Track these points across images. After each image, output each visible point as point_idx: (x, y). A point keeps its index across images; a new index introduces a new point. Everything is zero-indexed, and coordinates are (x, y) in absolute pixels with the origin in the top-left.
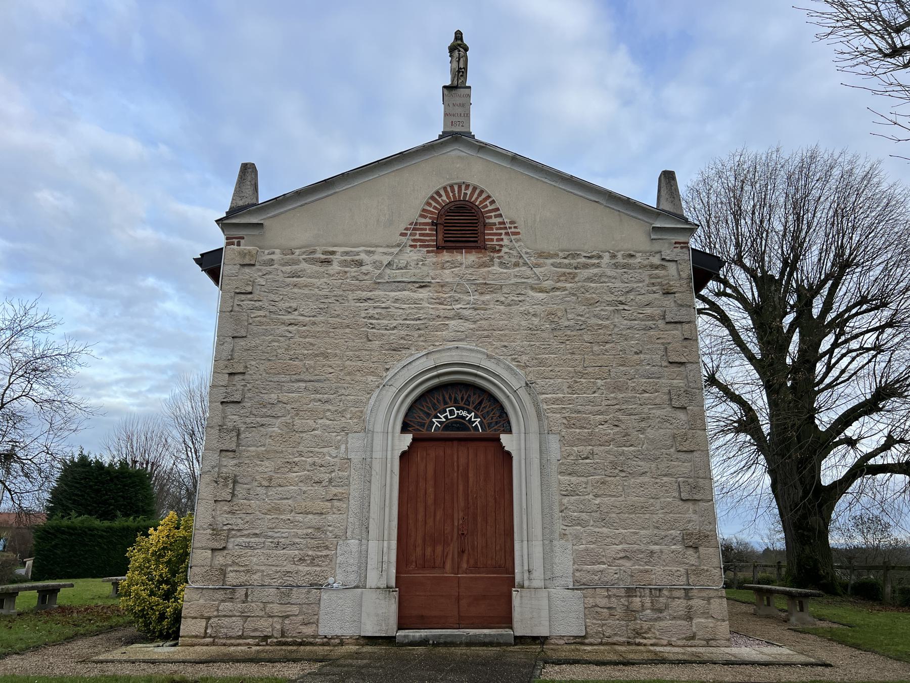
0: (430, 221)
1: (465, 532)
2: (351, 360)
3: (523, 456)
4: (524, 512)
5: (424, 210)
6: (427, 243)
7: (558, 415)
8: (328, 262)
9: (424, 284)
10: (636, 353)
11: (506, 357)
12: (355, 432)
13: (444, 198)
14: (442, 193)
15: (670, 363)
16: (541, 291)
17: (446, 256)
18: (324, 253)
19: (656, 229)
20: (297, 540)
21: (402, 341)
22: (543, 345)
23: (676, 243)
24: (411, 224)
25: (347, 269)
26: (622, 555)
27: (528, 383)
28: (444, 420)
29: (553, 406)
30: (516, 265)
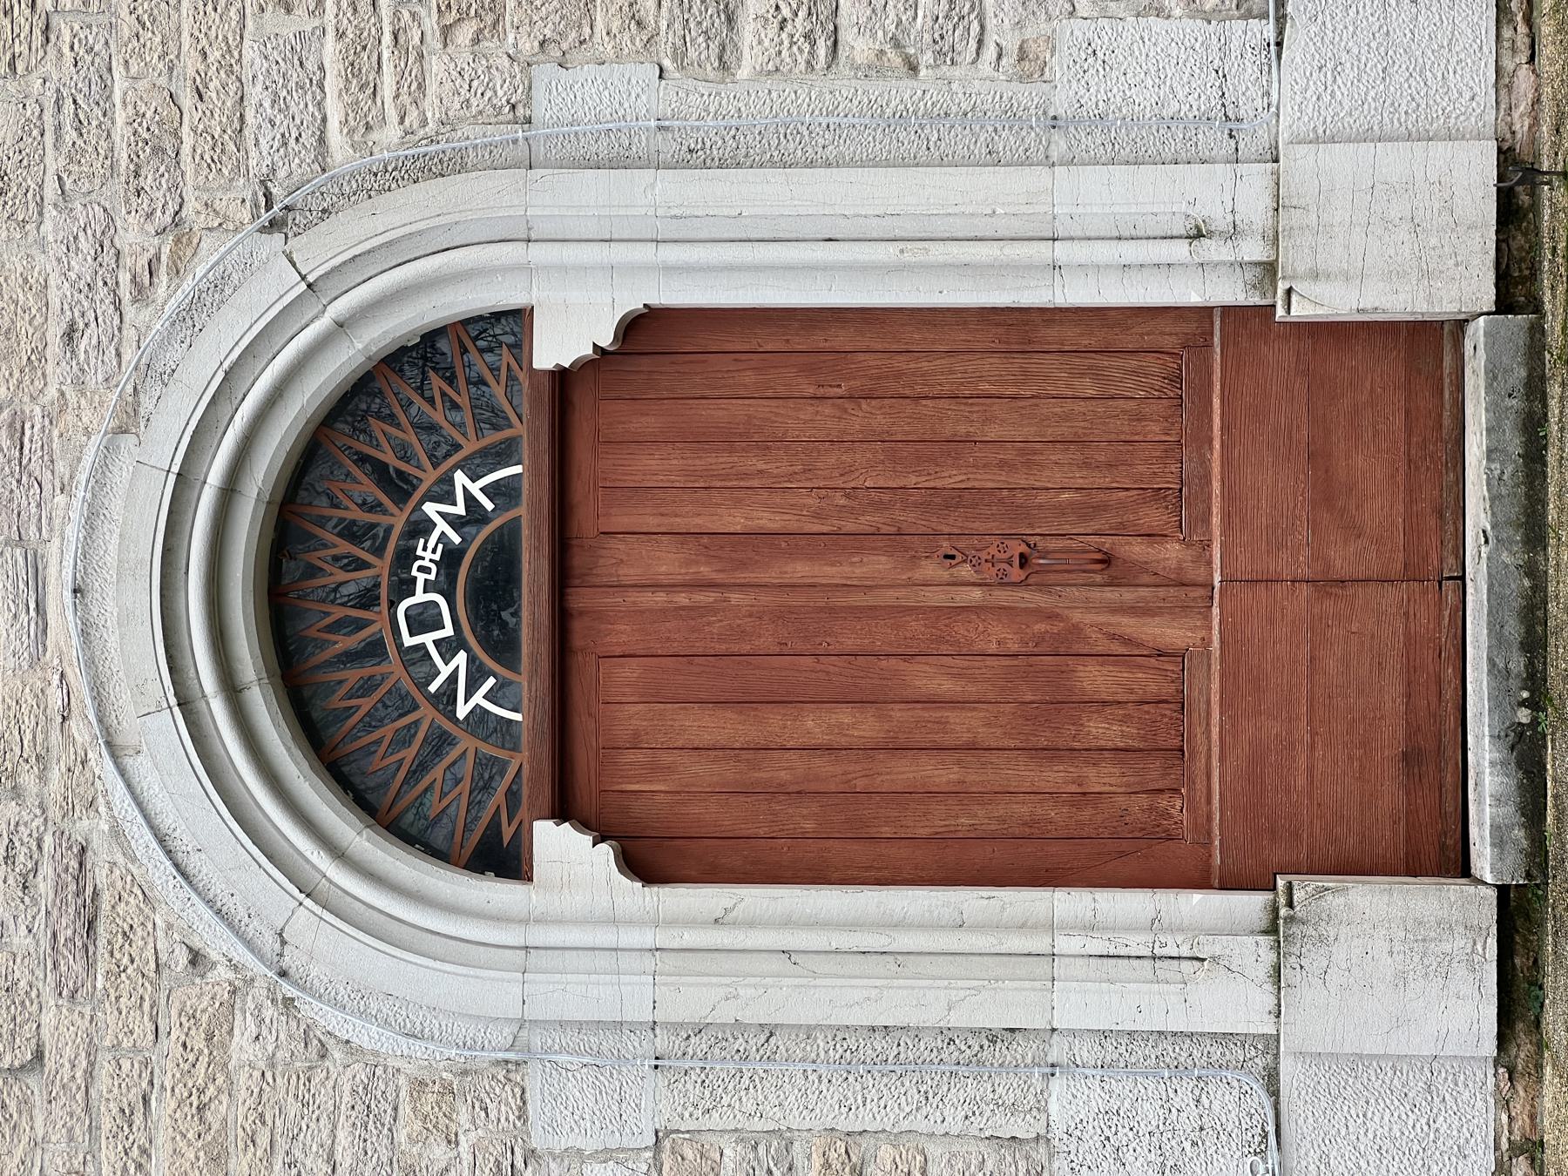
1: (1018, 548)
2: (144, 1151)
3: (645, 253)
4: (914, 253)
7: (436, 66)
11: (129, 333)
12: (522, 1115)
21: (44, 886)
22: (58, 137)
27: (265, 217)
28: (461, 659)
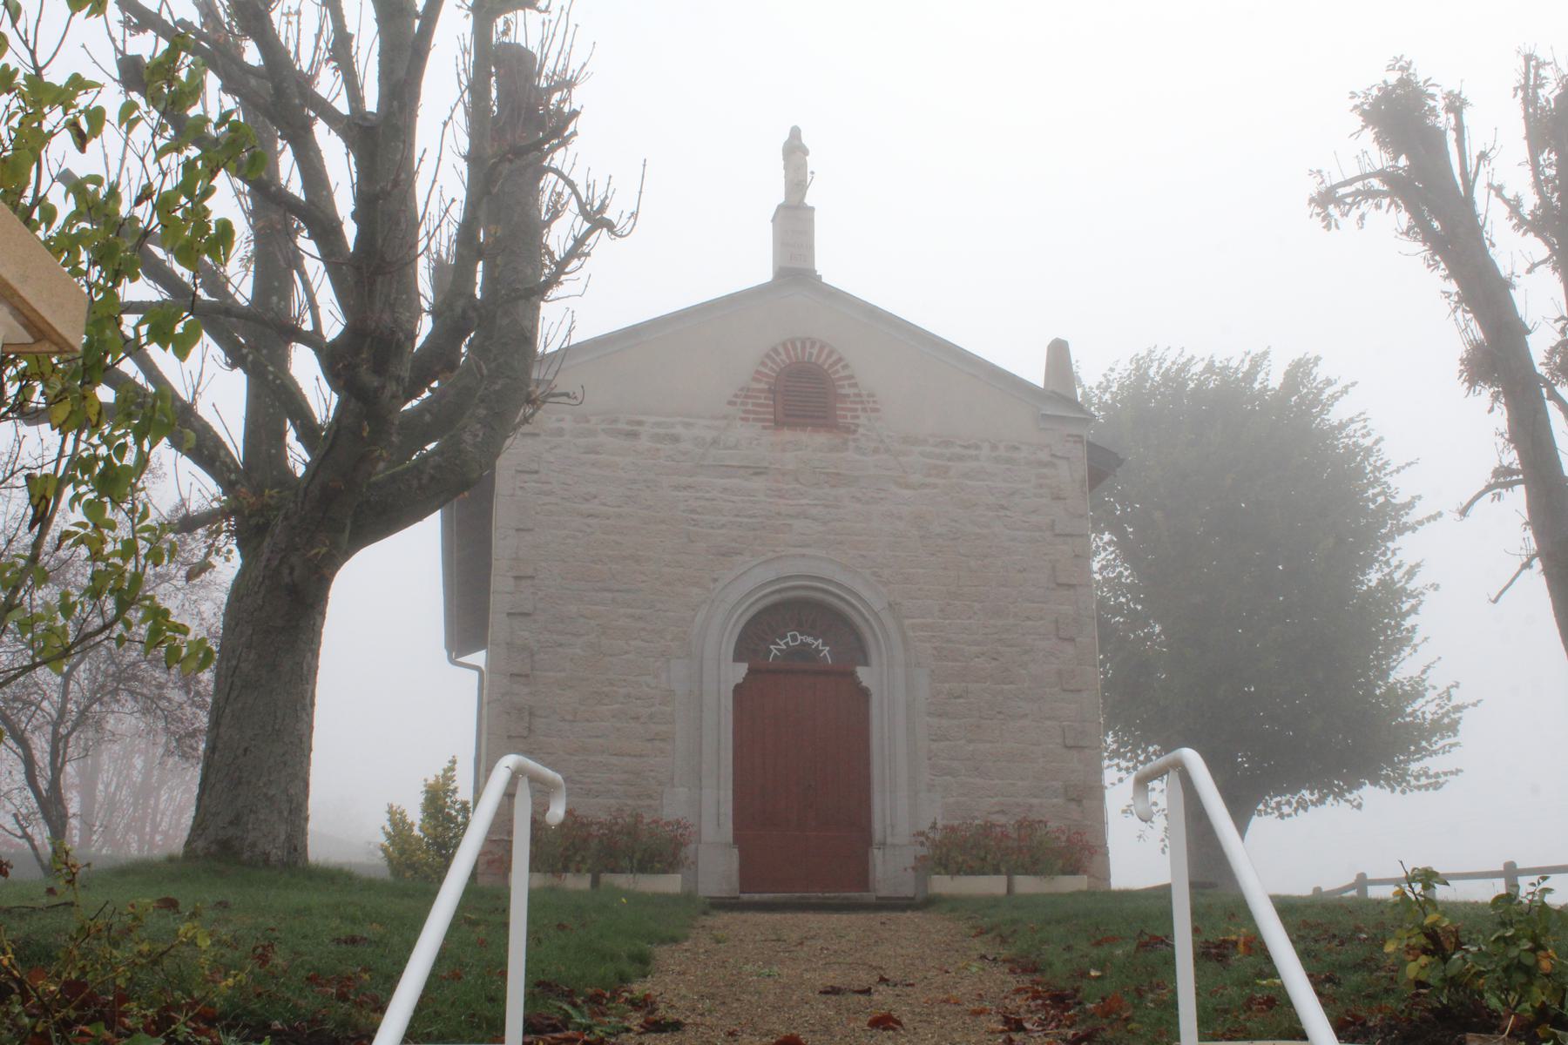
0: (766, 387)
5: (758, 372)
6: (762, 416)
8: (634, 435)
9: (759, 470)
10: (1020, 571)
13: (784, 357)
14: (781, 350)
15: (1059, 585)
16: (907, 486)
17: (787, 435)
18: (629, 423)
19: (1046, 417)
20: (614, 787)
23: (1069, 435)
24: (742, 389)
25: (659, 446)
26: (997, 808)
28: (784, 647)
29: (921, 633)
30: (876, 451)
